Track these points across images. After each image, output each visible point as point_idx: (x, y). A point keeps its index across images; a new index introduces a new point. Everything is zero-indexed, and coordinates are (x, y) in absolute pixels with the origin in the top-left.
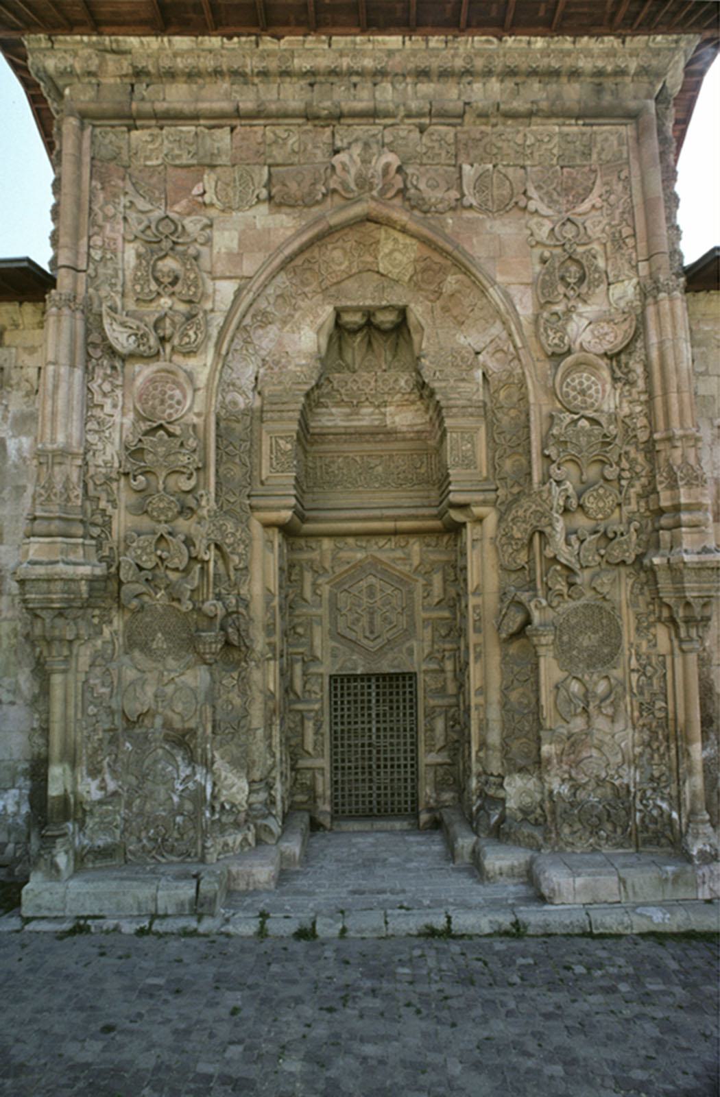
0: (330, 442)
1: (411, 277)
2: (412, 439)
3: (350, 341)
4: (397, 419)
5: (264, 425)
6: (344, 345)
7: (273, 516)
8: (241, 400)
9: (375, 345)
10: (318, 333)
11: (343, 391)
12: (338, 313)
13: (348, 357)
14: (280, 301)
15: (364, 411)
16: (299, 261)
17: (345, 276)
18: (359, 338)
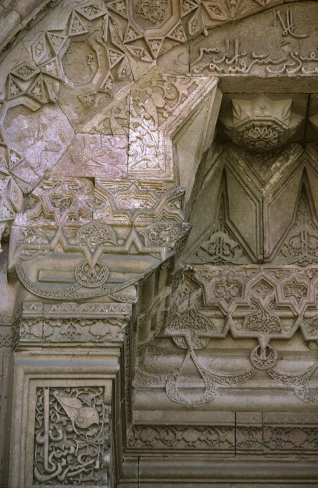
0: (191, 449)
3: (250, 180)
5: (18, 357)
6: (233, 189)
11: (231, 309)
14: (80, 53)
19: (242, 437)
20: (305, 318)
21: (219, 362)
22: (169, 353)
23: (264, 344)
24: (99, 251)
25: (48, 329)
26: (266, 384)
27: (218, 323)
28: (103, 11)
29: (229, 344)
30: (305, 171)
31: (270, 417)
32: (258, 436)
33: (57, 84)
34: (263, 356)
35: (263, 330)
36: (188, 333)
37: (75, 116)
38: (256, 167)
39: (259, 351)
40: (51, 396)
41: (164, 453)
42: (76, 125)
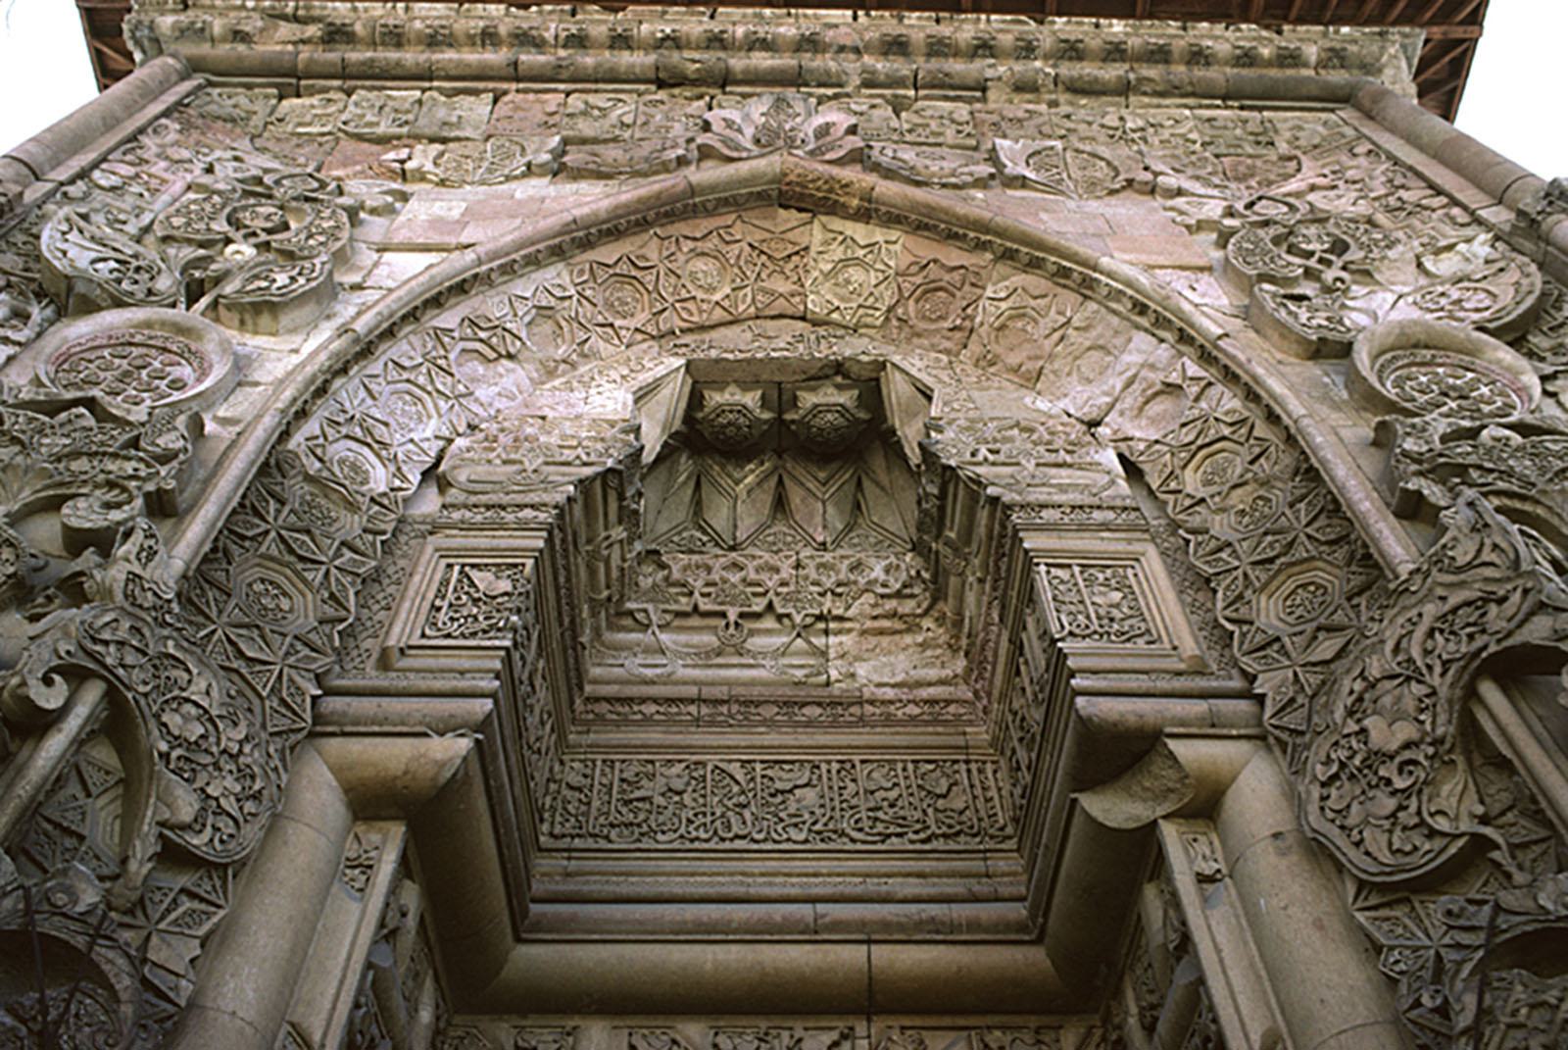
0: (647, 720)
1: (890, 310)
2: (913, 720)
3: (725, 482)
4: (862, 670)
5: (430, 538)
7: (392, 755)
8: (379, 479)
9: (796, 496)
10: (642, 396)
12: (701, 378)
13: (718, 517)
14: (547, 327)
15: (756, 643)
16: (608, 253)
17: (719, 315)
18: (751, 475)
19: (705, 710)
20: (777, 594)
21: (683, 638)
22: (632, 631)
23: (732, 616)
24: (540, 460)
25: (468, 514)
26: (735, 660)
27: (684, 600)
28: (573, 292)
29: (695, 621)
30: (780, 482)
31: (737, 691)
32: (724, 709)
33: (518, 343)
34: (732, 630)
35: (732, 604)
36: (650, 607)
37: (535, 375)
38: (730, 468)
39: (727, 626)
40: (461, 572)
41: (617, 724)
42: (536, 383)
